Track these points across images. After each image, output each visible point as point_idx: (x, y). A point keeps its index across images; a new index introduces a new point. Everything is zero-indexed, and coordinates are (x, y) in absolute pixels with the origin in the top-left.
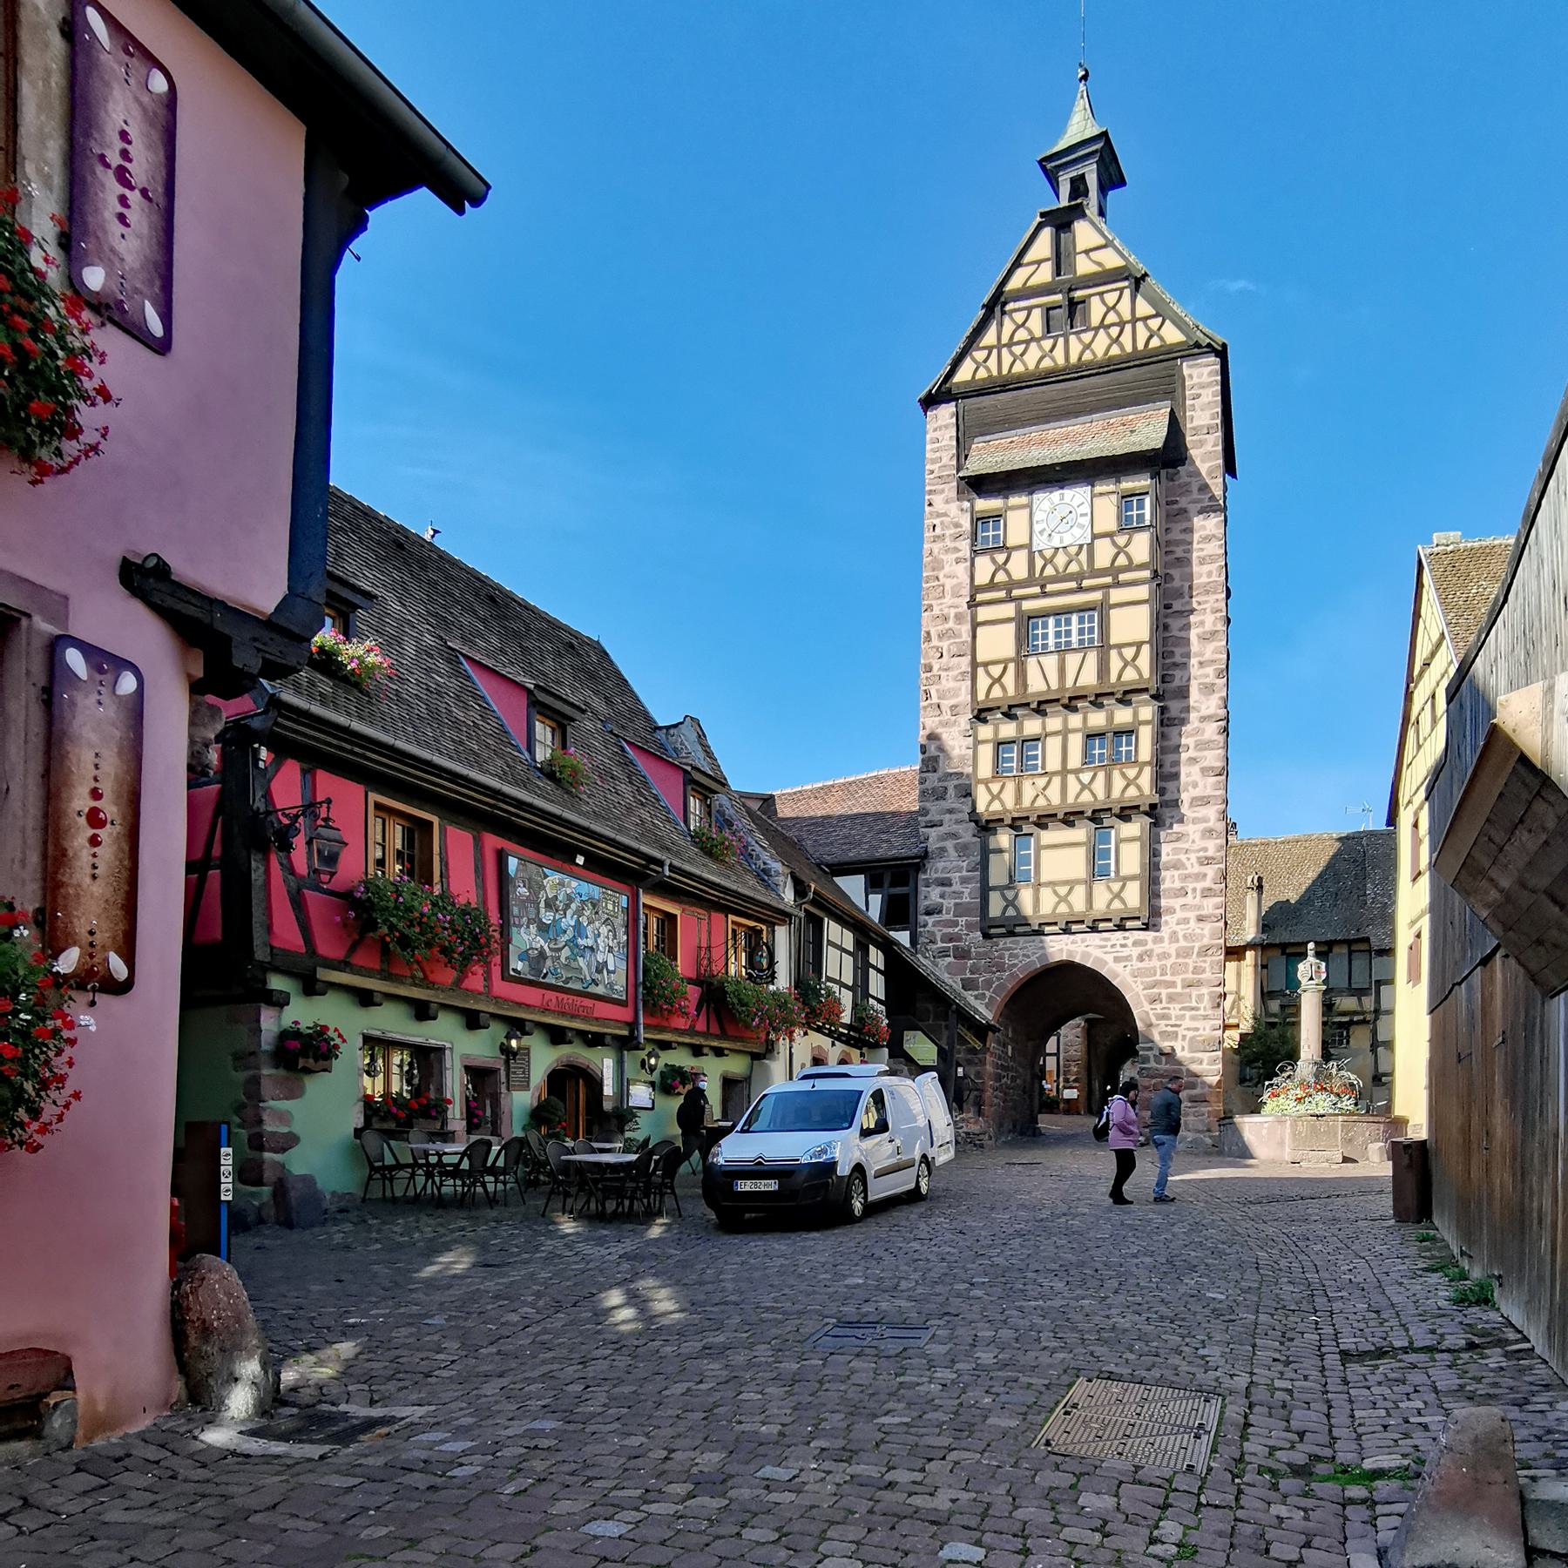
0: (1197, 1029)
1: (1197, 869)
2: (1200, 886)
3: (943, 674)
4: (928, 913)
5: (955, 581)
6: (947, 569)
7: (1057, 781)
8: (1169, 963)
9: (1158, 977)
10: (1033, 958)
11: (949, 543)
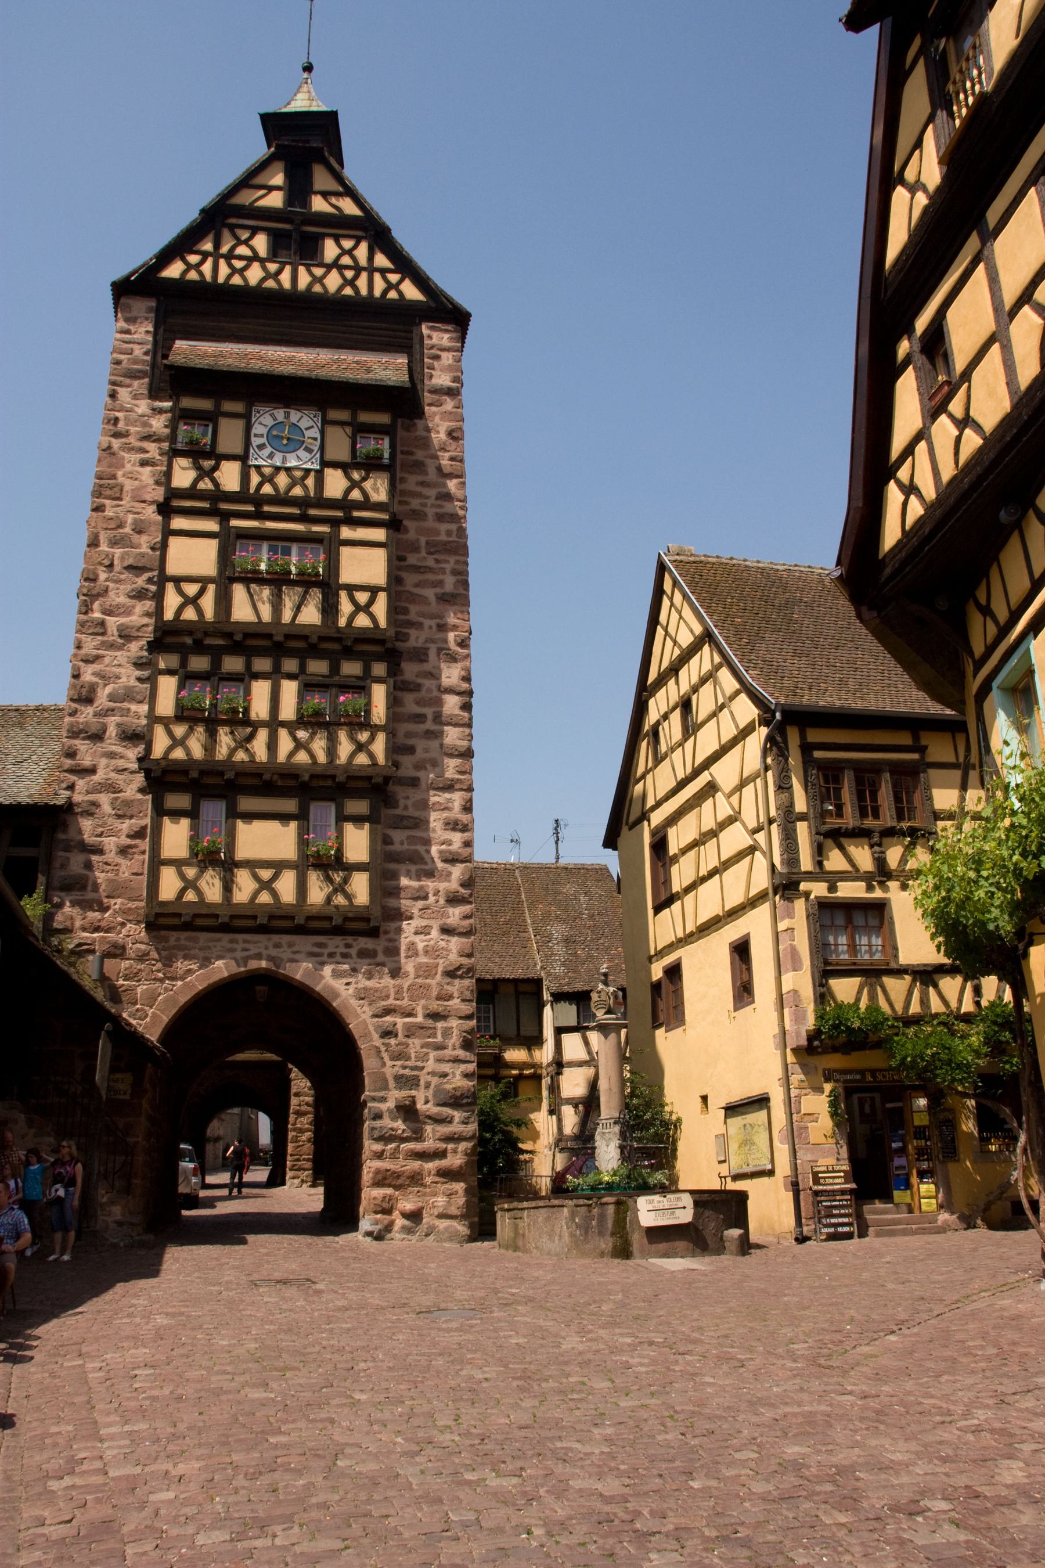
0: (445, 1075)
3: (111, 585)
6: (128, 467)
9: (391, 1001)
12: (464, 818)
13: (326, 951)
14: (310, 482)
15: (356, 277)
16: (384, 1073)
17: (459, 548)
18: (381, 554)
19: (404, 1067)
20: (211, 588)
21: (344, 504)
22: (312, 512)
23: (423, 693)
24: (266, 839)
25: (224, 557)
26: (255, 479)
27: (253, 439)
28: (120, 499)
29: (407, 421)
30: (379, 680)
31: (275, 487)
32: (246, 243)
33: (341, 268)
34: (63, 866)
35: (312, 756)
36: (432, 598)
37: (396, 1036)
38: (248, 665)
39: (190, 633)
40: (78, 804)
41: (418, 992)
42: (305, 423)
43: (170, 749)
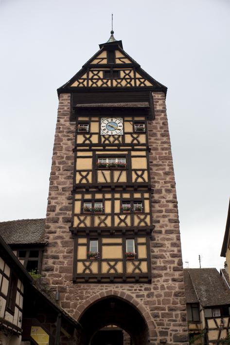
0: (177, 331)
1: (170, 259)
2: (172, 266)
3: (60, 176)
4: (47, 270)
5: (67, 146)
6: (64, 141)
7: (109, 218)
8: (161, 299)
9: (157, 305)
10: (98, 294)
11: (65, 133)
12: (177, 242)
13: (133, 289)
14: (120, 139)
15: (131, 81)
16: (155, 331)
17: (169, 158)
18: (145, 160)
19: (162, 328)
20: (91, 173)
21: (132, 145)
22: (121, 148)
23: (161, 203)
24: (112, 251)
25: (94, 163)
26: (103, 139)
27: (101, 128)
28: (61, 150)
29: (150, 122)
30: (147, 199)
31: (109, 141)
32: (96, 75)
33: (126, 79)
34: (46, 263)
35: (126, 224)
36: (162, 174)
37: (159, 317)
38: (104, 196)
39: (84, 188)
40: (50, 243)
41: (166, 302)
42: (117, 122)
43: (79, 224)
